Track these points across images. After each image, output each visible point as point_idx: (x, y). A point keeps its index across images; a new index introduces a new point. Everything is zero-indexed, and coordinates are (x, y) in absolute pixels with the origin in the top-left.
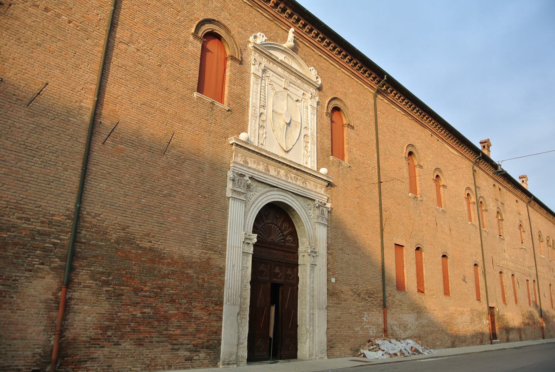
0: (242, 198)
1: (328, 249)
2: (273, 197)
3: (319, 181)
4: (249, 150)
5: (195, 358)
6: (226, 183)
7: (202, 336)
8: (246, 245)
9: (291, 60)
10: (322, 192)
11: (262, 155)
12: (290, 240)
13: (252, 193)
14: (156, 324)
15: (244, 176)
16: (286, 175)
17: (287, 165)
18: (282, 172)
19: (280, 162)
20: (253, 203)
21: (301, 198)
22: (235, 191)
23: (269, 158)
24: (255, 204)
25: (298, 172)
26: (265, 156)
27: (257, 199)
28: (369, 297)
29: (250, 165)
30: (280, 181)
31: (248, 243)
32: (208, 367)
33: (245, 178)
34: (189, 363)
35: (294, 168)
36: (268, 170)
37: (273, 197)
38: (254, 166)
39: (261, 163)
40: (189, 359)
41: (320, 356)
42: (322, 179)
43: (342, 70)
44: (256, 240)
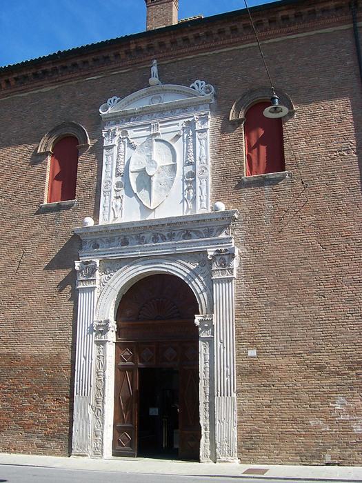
1: (239, 309)
5: (47, 446)
7: (52, 425)
9: (162, 96)
14: (12, 415)
15: (91, 261)
28: (350, 369)
32: (58, 455)
34: (41, 450)
40: (42, 446)
41: (223, 458)
43: (267, 42)
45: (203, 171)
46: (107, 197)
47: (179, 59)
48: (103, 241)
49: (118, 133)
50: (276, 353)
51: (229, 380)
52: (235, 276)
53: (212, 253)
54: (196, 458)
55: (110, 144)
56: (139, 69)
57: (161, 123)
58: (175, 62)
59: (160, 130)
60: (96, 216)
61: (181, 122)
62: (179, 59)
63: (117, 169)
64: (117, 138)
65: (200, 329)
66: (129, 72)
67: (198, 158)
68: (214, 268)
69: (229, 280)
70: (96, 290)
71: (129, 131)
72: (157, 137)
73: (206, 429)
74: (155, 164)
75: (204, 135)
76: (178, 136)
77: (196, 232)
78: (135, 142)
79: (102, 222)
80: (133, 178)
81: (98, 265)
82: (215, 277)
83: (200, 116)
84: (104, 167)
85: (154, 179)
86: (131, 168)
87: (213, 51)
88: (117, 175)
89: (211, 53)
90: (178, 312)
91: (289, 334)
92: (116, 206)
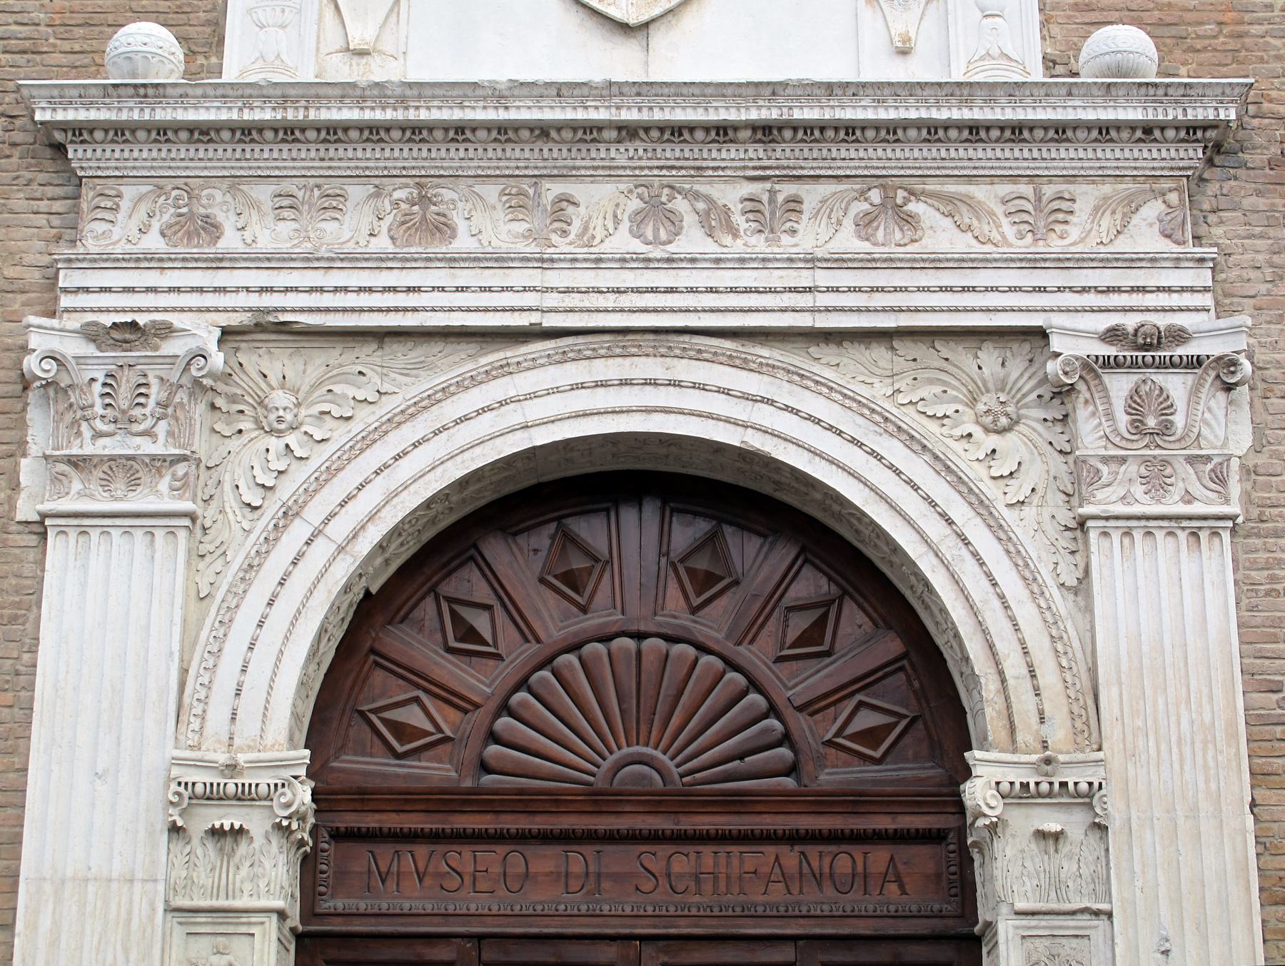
0: (158, 496)
2: (513, 416)
3: (1065, 157)
4: (202, 133)
6: (22, 425)
8: (207, 853)
10: (1144, 235)
11: (333, 132)
12: (871, 736)
13: (292, 439)
15: (166, 331)
16: (656, 213)
17: (628, 131)
18: (601, 202)
19: (542, 131)
20: (290, 514)
21: (879, 353)
22: (77, 463)
23: (416, 132)
24: (315, 512)
25: (784, 154)
26: (374, 132)
27: (331, 472)
29: (230, 242)
30: (555, 278)
31: (217, 833)
33: (173, 347)
35: (723, 132)
36: (443, 229)
37: (513, 416)
38: (271, 235)
39: (356, 192)
42: (1104, 131)
44: (303, 795)
48: (254, 205)
52: (1234, 509)
60: (204, 39)
77: (950, 205)
79: (237, 63)
82: (1104, 501)
90: (786, 739)
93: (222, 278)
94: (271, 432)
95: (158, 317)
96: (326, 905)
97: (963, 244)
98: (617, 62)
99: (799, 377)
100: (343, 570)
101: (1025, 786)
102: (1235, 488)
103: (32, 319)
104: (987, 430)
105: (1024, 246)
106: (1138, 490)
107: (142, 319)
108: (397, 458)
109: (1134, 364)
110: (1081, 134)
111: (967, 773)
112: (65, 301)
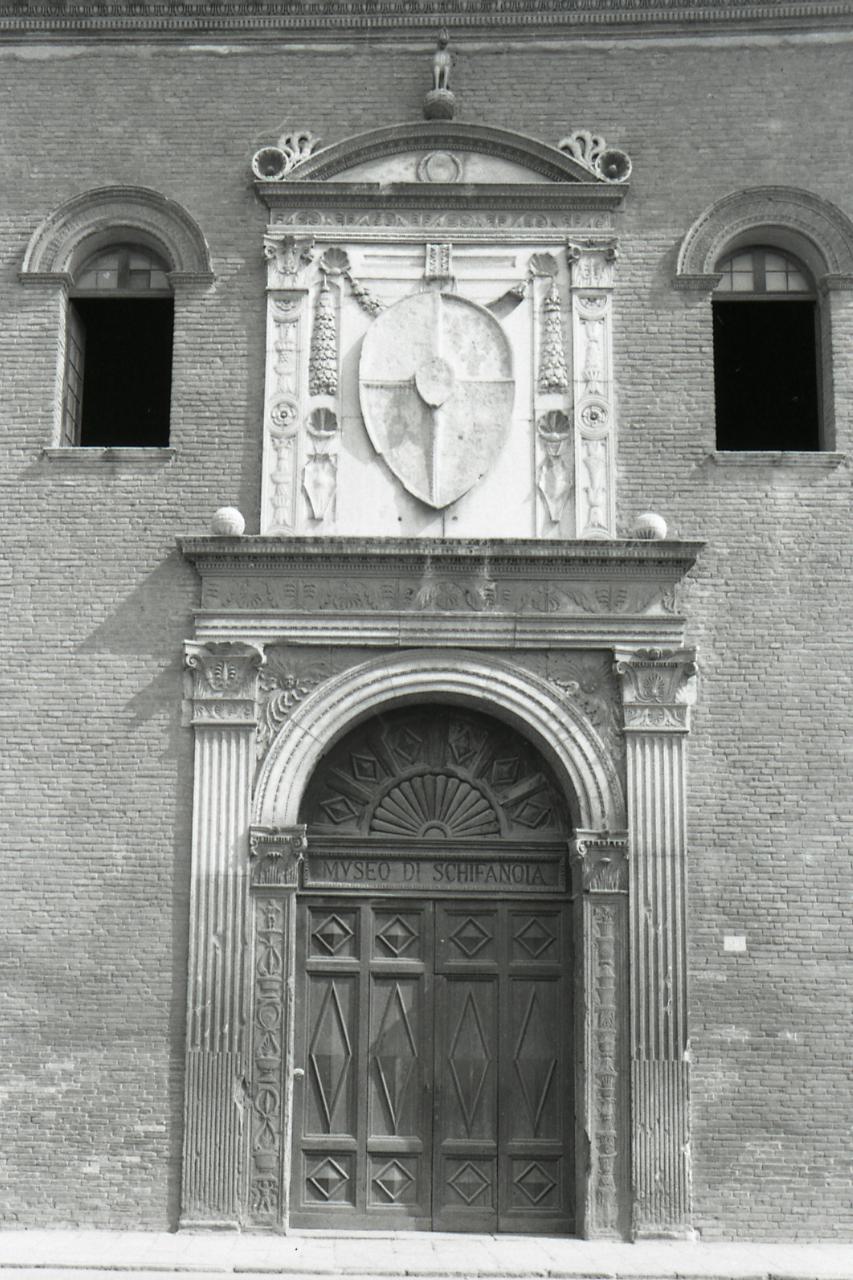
13: (294, 692)
45: (594, 417)
46: (285, 453)
47: (519, 45)
49: (317, 253)
50: (801, 947)
51: (671, 1015)
53: (626, 659)
54: (571, 1227)
55: (288, 284)
56: (381, 53)
57: (456, 245)
58: (498, 53)
59: (454, 270)
60: (253, 514)
61: (523, 255)
62: (519, 45)
63: (313, 369)
64: (313, 268)
65: (587, 869)
66: (340, 54)
67: (578, 376)
68: (629, 696)
69: (674, 737)
70: (253, 736)
71: (355, 254)
72: (447, 290)
73: (602, 1149)
74: (443, 375)
75: (591, 311)
76: (513, 299)
78: (375, 292)
80: (376, 409)
81: (264, 659)
82: (636, 723)
83: (585, 244)
84: (271, 359)
85: (440, 417)
86: (367, 372)
87: (626, 37)
88: (321, 387)
89: (622, 44)
91: (837, 899)
92: (317, 485)
93: (264, 623)
94: (286, 688)
95: (239, 640)
96: (310, 883)
97: (579, 613)
98: (431, 530)
99: (504, 668)
100: (317, 749)
101: (596, 843)
102: (688, 720)
103: (186, 641)
104: (586, 692)
105: (603, 613)
106: (647, 720)
107: (232, 642)
108: (339, 701)
109: (649, 666)
110: (632, 563)
111: (573, 836)
112: (198, 633)
